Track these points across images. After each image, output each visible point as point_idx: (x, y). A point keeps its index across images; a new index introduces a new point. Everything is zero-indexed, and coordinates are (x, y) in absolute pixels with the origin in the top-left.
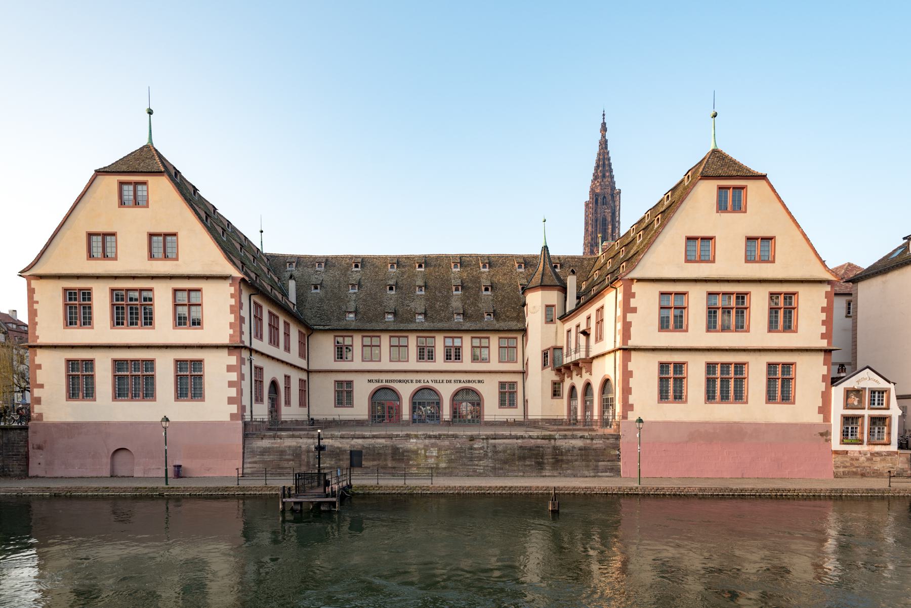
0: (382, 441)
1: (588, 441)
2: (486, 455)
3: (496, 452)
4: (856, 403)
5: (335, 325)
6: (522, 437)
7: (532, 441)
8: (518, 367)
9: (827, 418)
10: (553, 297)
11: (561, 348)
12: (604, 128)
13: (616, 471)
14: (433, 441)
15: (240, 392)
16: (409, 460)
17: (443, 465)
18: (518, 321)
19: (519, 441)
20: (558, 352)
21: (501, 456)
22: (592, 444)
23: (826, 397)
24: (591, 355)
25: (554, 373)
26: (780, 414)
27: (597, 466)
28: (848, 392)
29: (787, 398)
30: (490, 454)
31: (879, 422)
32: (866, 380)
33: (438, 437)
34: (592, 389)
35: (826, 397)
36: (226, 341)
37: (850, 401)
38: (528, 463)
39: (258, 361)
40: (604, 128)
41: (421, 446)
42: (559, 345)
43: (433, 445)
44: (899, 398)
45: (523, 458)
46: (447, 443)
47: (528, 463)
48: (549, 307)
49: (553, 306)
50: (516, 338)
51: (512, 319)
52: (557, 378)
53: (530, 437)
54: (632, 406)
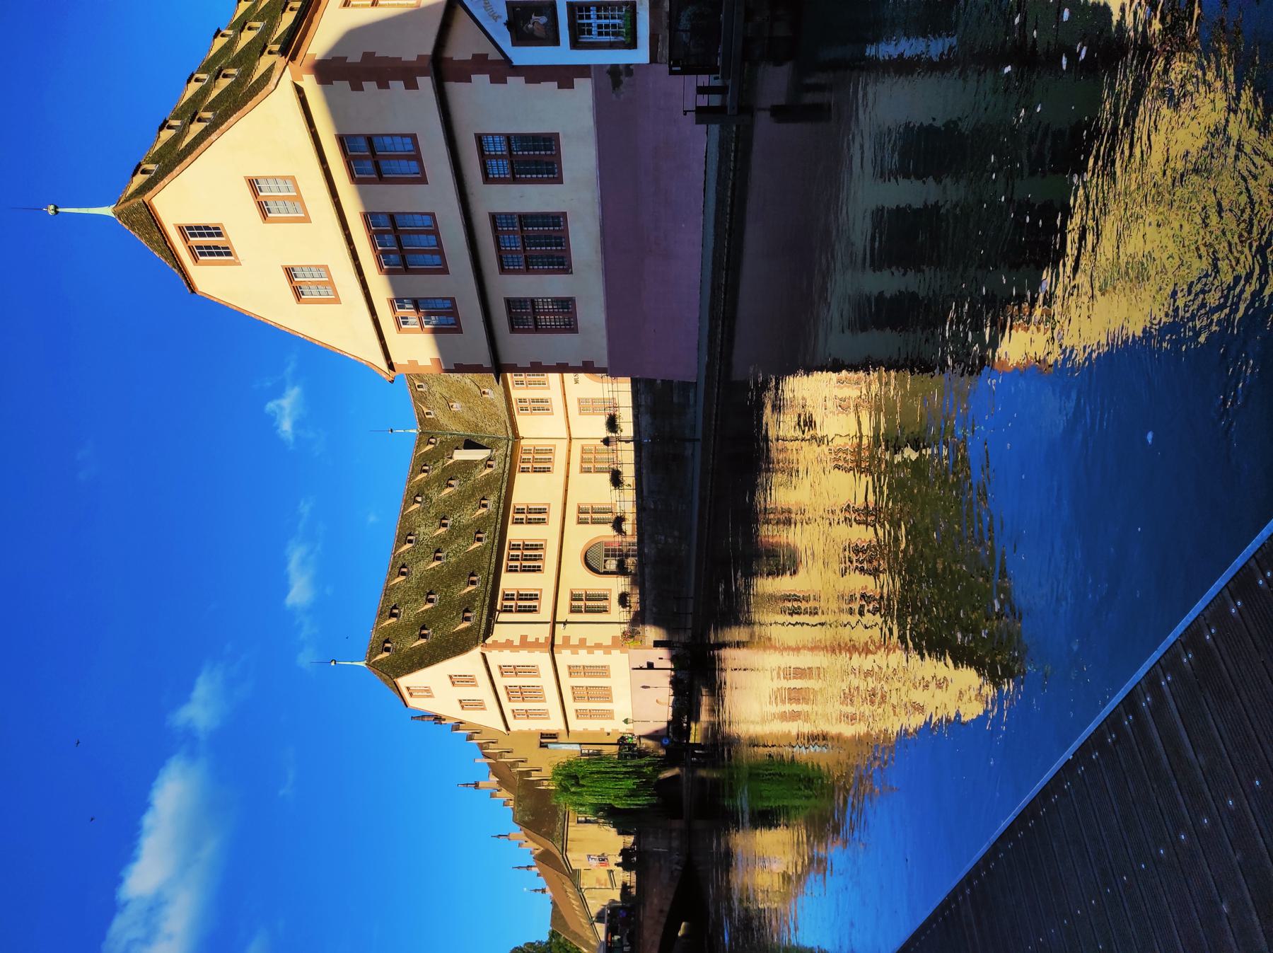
1: (642, 409)
4: (543, 20)
5: (504, 416)
7: (644, 460)
13: (685, 386)
15: (598, 646)
17: (676, 533)
23: (535, 74)
26: (580, 158)
28: (521, 37)
29: (549, 142)
35: (535, 74)
36: (547, 656)
37: (539, 33)
39: (563, 614)
54: (584, 363)
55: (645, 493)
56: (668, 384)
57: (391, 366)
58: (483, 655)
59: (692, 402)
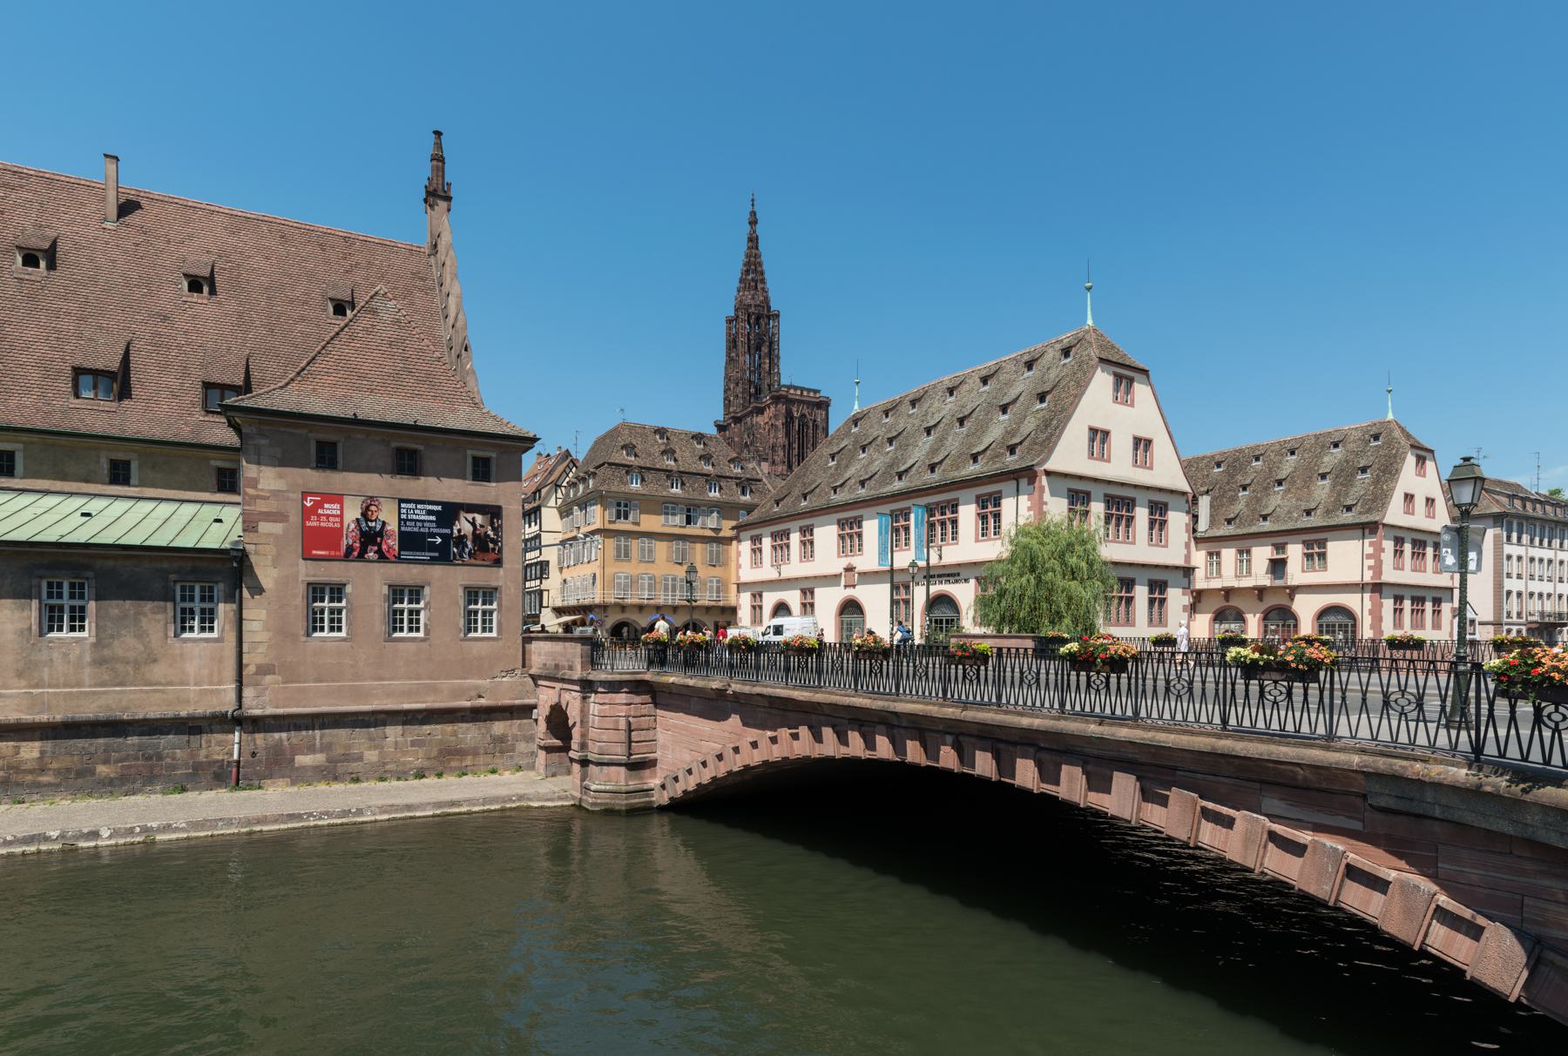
12: (753, 222)
24: (1295, 583)
34: (1295, 618)
40: (753, 222)
58: (1184, 493)
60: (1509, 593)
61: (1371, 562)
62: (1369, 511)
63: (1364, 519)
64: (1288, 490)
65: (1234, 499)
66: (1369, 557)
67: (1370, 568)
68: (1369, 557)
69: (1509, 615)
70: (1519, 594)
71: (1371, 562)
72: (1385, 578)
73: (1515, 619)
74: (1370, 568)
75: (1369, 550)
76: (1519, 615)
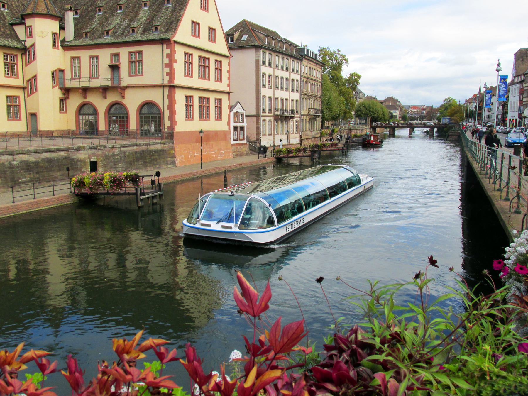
0: (62, 154)
1: (163, 146)
2: (121, 159)
3: (125, 157)
6: (136, 145)
7: (141, 147)
8: (18, 82)
9: (229, 128)
10: (53, 26)
11: (62, 71)
14: (93, 151)
16: (81, 168)
18: (15, 40)
19: (135, 148)
20: (60, 74)
21: (128, 160)
22: (164, 147)
24: (123, 84)
25: (60, 91)
27: (167, 161)
30: (123, 158)
31: (242, 128)
32: (238, 109)
33: (95, 148)
38: (140, 163)
41: (87, 156)
42: (62, 68)
43: (94, 155)
44: (246, 116)
45: (137, 160)
46: (100, 152)
47: (140, 163)
48: (54, 35)
49: (57, 34)
50: (16, 55)
51: (9, 36)
52: (62, 96)
53: (140, 145)
55: (122, 149)
56: (174, 155)
57: (175, 42)
59: (170, 166)
60: (264, 97)
61: (167, 70)
62: (167, 31)
63: (163, 36)
64: (124, 14)
65: (92, 18)
66: (167, 65)
67: (167, 74)
68: (167, 65)
69: (264, 110)
70: (270, 98)
71: (167, 70)
72: (177, 82)
73: (267, 114)
74: (167, 74)
75: (166, 61)
76: (270, 110)
